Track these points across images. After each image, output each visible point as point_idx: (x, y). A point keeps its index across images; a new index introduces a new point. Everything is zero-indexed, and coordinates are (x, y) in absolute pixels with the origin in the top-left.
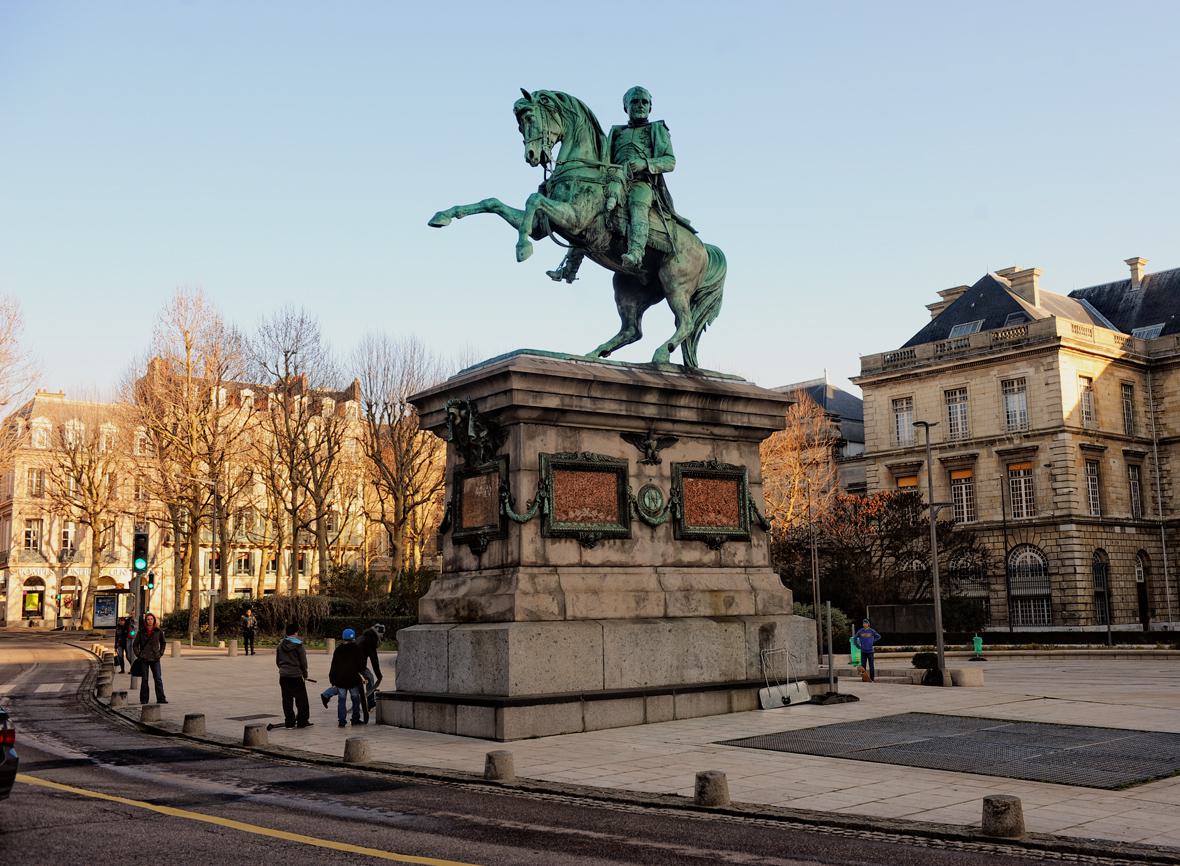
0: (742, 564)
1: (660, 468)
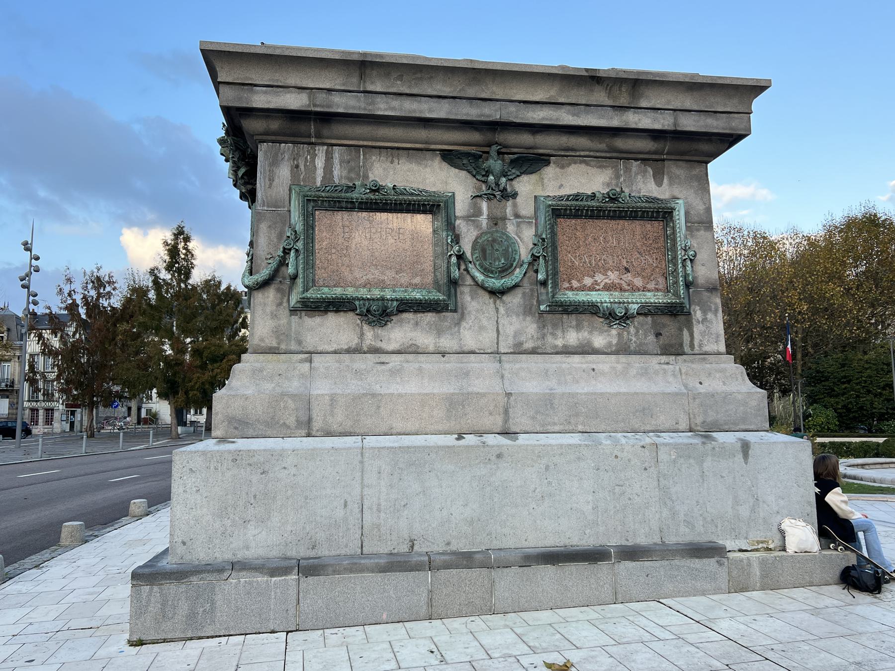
1: (515, 205)
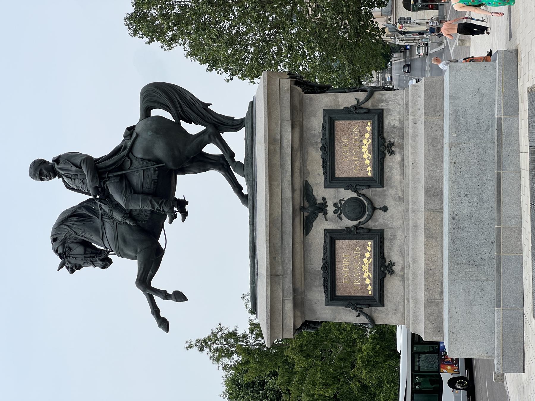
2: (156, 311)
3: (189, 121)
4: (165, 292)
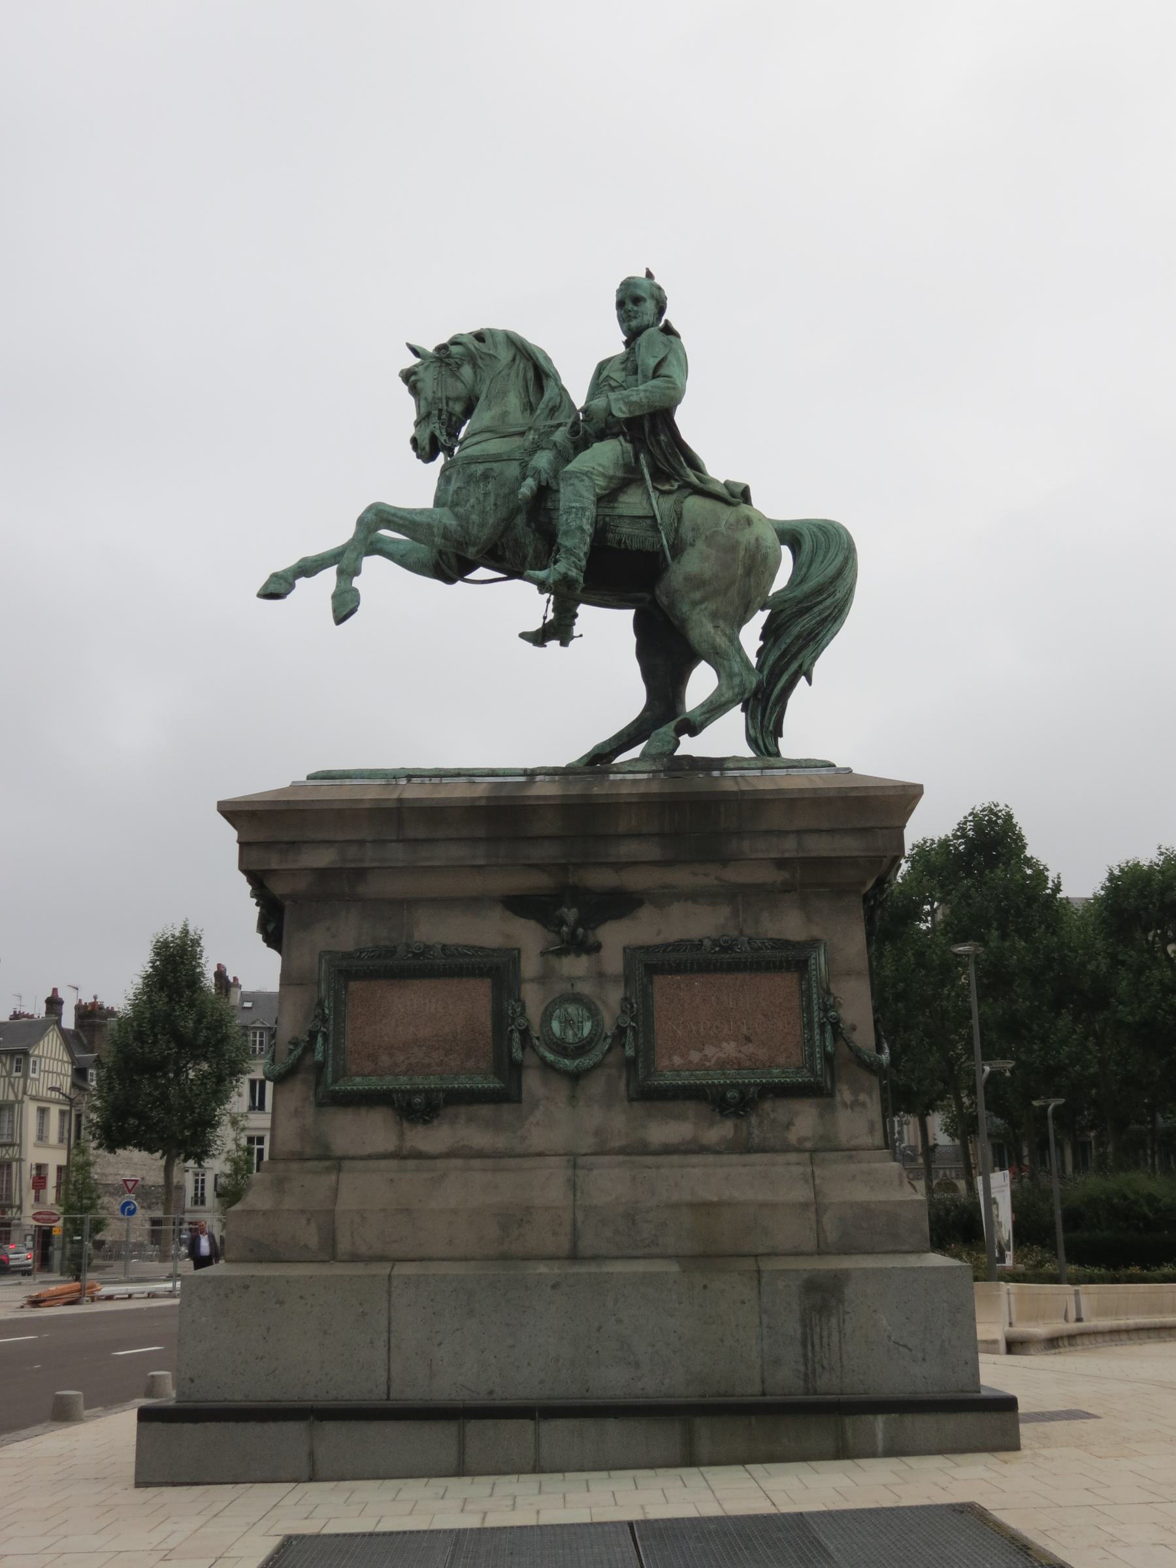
0: (808, 1145)
2: (308, 568)
3: (769, 633)
4: (357, 572)
